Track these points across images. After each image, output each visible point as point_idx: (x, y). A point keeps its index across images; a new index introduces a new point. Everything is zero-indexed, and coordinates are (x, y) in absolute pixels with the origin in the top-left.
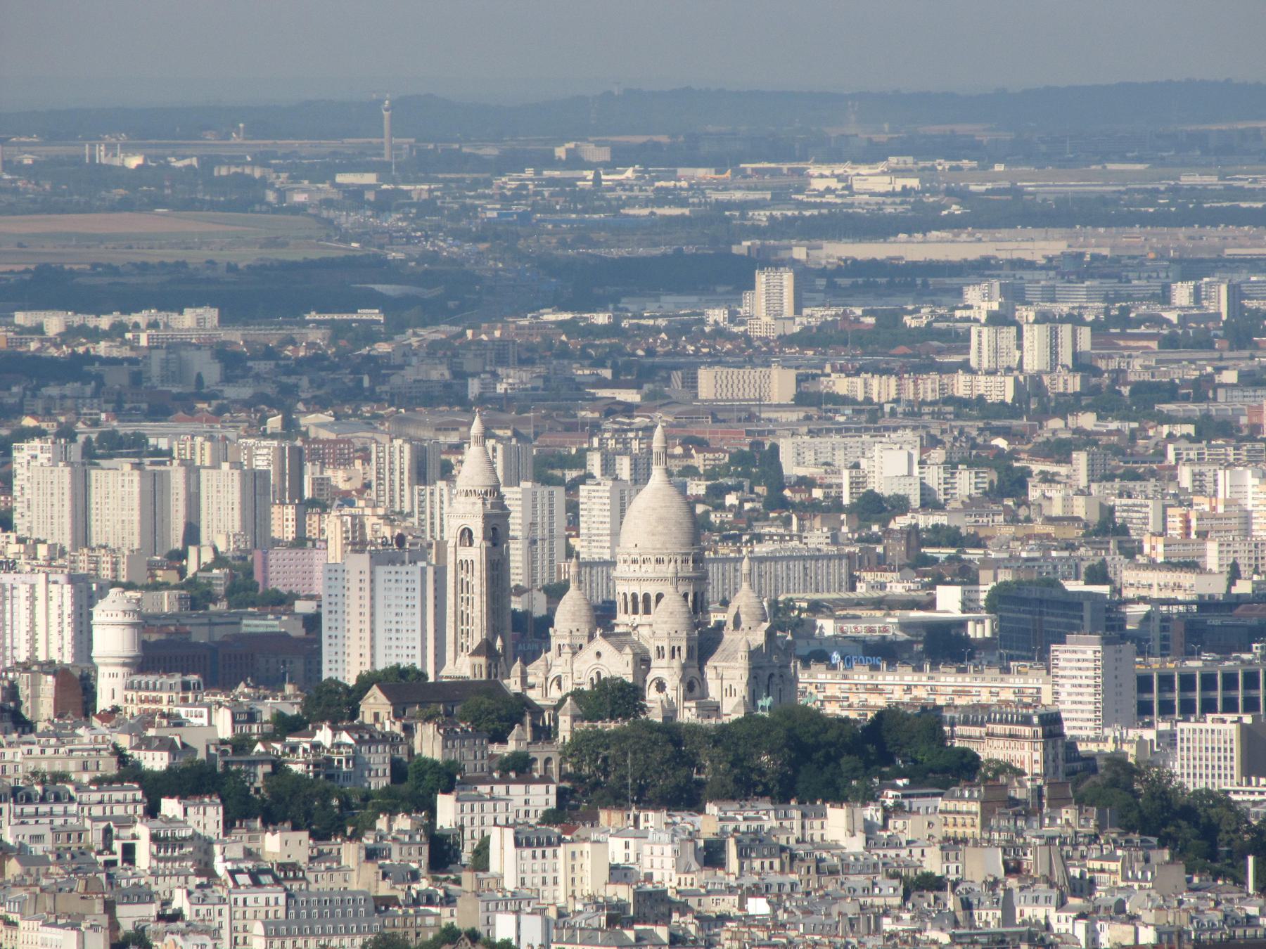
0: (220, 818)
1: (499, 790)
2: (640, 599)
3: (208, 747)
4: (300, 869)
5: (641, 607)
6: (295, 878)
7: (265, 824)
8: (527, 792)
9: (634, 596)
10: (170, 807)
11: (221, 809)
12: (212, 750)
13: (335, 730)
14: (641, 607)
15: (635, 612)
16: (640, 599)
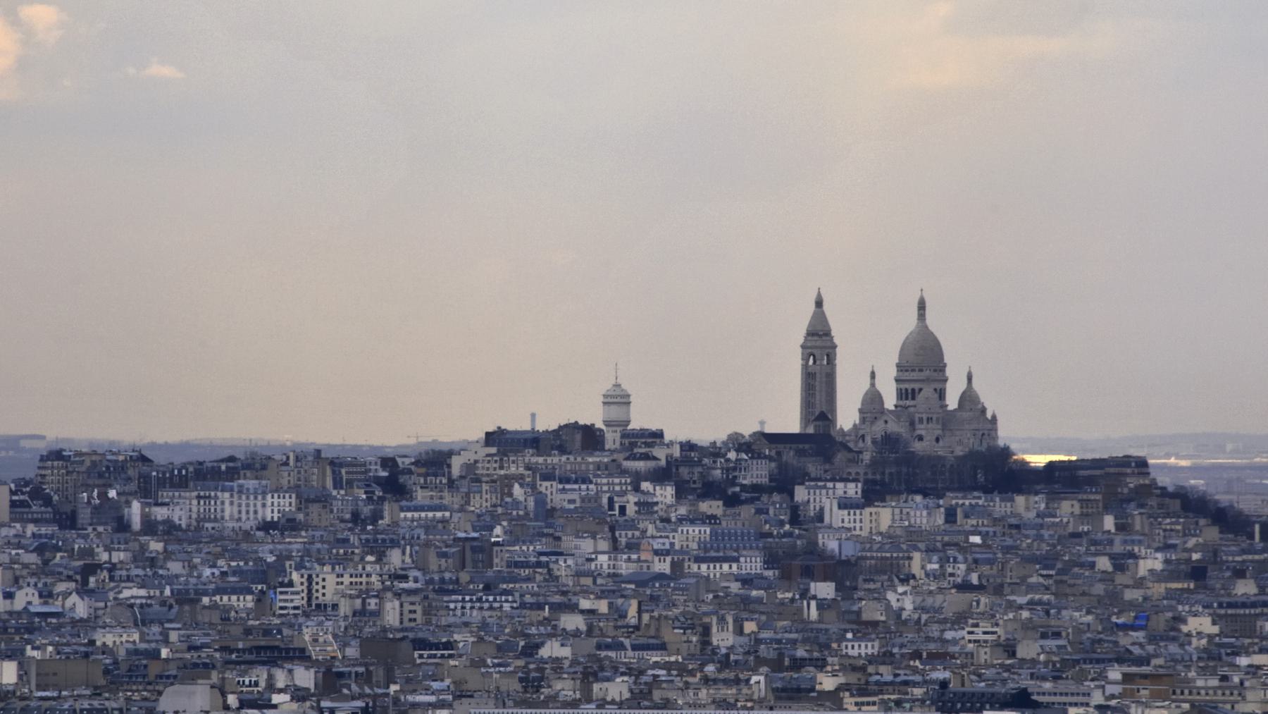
0: (674, 492)
2: (910, 391)
4: (719, 519)
5: (910, 396)
6: (715, 523)
7: (699, 496)
8: (845, 487)
14: (910, 396)
16: (910, 391)
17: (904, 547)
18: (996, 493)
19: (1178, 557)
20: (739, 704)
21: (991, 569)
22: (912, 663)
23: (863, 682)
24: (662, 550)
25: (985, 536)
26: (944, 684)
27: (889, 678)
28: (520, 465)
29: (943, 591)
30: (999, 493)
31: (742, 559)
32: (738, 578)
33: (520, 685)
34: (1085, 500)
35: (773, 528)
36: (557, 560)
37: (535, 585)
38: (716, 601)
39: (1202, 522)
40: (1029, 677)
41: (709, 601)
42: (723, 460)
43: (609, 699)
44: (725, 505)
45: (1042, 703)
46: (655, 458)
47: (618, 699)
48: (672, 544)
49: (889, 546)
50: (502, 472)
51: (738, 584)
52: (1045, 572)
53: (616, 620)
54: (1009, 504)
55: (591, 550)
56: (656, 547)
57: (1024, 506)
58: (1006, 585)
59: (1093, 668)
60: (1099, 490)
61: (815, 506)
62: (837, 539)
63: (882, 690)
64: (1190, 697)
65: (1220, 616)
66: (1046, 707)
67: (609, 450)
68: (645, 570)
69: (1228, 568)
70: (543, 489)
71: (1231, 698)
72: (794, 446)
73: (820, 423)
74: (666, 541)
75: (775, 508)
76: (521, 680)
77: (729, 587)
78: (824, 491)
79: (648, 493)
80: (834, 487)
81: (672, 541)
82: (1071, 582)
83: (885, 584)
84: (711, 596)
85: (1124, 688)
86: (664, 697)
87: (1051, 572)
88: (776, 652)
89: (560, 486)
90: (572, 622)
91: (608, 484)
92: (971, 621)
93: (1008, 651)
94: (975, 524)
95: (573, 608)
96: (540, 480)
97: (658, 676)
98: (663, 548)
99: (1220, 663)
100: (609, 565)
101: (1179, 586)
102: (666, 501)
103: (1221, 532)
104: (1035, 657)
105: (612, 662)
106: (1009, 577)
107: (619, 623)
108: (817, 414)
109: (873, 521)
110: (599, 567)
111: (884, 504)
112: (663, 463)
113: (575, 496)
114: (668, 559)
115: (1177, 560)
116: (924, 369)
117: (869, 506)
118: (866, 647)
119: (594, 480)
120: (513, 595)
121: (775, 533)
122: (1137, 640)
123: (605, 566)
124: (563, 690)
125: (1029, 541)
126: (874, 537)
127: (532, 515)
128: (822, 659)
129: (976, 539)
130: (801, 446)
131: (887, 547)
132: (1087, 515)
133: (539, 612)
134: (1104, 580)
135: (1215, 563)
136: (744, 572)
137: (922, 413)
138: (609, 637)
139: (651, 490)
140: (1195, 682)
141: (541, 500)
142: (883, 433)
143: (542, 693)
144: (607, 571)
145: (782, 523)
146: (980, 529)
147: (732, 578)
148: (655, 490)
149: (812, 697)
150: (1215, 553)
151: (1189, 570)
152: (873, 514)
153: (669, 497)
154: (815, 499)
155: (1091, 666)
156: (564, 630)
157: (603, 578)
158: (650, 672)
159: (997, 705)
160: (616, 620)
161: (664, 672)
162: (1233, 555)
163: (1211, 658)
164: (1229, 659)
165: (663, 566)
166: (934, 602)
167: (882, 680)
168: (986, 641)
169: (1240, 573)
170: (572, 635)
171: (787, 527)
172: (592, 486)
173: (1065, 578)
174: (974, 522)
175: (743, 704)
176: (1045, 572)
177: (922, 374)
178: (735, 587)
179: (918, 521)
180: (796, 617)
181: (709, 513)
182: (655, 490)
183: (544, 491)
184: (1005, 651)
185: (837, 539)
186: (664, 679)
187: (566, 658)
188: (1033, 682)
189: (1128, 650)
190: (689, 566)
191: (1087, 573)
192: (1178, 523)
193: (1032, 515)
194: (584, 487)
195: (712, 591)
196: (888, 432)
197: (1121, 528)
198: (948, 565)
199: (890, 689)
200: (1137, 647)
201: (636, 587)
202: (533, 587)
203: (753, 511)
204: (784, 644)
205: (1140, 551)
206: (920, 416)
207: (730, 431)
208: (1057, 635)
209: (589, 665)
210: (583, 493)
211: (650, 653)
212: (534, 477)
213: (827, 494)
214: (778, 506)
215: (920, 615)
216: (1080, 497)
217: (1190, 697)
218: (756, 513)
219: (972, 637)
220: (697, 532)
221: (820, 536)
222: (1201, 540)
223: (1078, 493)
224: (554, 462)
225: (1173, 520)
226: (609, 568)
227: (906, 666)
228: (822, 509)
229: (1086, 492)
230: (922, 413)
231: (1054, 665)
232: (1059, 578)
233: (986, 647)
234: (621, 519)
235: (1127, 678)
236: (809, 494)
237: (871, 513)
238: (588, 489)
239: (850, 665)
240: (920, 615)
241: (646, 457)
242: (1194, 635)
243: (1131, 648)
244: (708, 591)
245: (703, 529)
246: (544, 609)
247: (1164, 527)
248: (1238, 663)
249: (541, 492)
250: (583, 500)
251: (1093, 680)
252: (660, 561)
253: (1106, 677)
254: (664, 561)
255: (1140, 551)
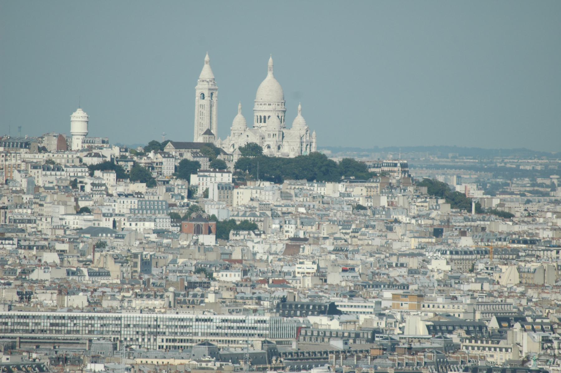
0: (115, 178)
1: (213, 174)
2: (263, 117)
3: (111, 156)
4: (143, 194)
5: (263, 120)
6: (141, 197)
7: (131, 180)
8: (222, 176)
9: (261, 117)
10: (98, 173)
11: (115, 174)
12: (112, 157)
13: (156, 153)
14: (263, 120)
15: (261, 122)
16: (263, 117)
17: (258, 214)
18: (315, 181)
19: (426, 223)
20: (156, 310)
21: (312, 228)
22: (263, 286)
23: (233, 297)
24: (108, 214)
25: (308, 208)
26: (284, 300)
27: (249, 295)
28: (18, 159)
29: (282, 241)
30: (317, 181)
31: (157, 220)
32: (155, 231)
33: (18, 297)
34: (369, 187)
35: (177, 201)
36: (41, 219)
37: (27, 234)
38: (141, 246)
39: (441, 201)
40: (335, 295)
41: (137, 245)
42: (146, 158)
43: (75, 306)
44: (147, 186)
45: (344, 312)
46: (103, 156)
47: (80, 307)
48: (114, 210)
49: (249, 213)
50: (7, 163)
51: (156, 235)
52: (344, 231)
53: (78, 257)
54: (323, 188)
55: (63, 213)
56: (104, 211)
57: (514, 196)
58: (321, 239)
59: (374, 290)
60: (378, 181)
61: (203, 188)
62: (217, 208)
63: (245, 302)
64: (433, 309)
65: (452, 260)
66: (346, 314)
67: (75, 151)
68: (96, 226)
69: (456, 229)
70: (32, 174)
71: (458, 310)
72: (190, 150)
73: (207, 136)
74: (109, 207)
75: (179, 188)
76: (18, 293)
77: (149, 237)
78: (209, 179)
79: (99, 178)
80: (215, 176)
81: (113, 207)
82: (361, 237)
83: (246, 237)
84: (138, 243)
85: (393, 303)
86: (110, 305)
87: (348, 231)
88: (179, 278)
89: (44, 173)
90: (50, 257)
91: (74, 171)
92: (299, 261)
93: (322, 279)
94: (302, 200)
95: (51, 248)
96: (31, 168)
97: (105, 292)
98: (108, 212)
99: (451, 289)
100: (74, 222)
101: (427, 240)
102: (109, 183)
103: (452, 208)
104: (339, 283)
105: (76, 283)
106: (322, 233)
107: (81, 259)
108: (205, 130)
109: (239, 197)
110: (67, 224)
111: (246, 187)
112: (108, 159)
113: (52, 179)
114: (112, 219)
115: (424, 224)
116: (272, 104)
117: (237, 188)
118: (235, 275)
119: (65, 169)
120: (13, 240)
121: (178, 204)
122: (401, 274)
123: (71, 223)
124: (46, 300)
125: (335, 211)
126: (240, 208)
127: (25, 190)
128: (208, 283)
129: (302, 210)
130: (195, 150)
131: (248, 214)
132: (370, 197)
133: (30, 251)
134: (381, 236)
135: (448, 226)
136: (158, 228)
137: (270, 131)
138: (74, 267)
139: (101, 176)
140: (436, 300)
141: (31, 182)
142: (246, 144)
143: (32, 302)
144: (73, 226)
145: (183, 198)
146: (305, 203)
147: (152, 232)
148: (103, 176)
149: (202, 306)
150: (448, 221)
151: (433, 231)
152: (239, 193)
153: (112, 180)
154: (203, 183)
155: (373, 289)
156: (46, 262)
157: (71, 230)
158: (100, 290)
159: (316, 313)
160: (78, 257)
161: (109, 290)
162: (459, 222)
163: (446, 285)
164: (457, 286)
165: (107, 224)
166: (277, 249)
167: (245, 296)
168: (308, 273)
169: (463, 233)
170: (50, 266)
171: (186, 200)
172: (63, 173)
173: (356, 235)
174: (301, 199)
175: (159, 310)
176: (344, 231)
177: (271, 107)
178: (153, 237)
179: (267, 198)
180: (191, 257)
181: (137, 191)
182: (103, 176)
183: (33, 175)
184: (320, 279)
185: (217, 208)
186: (109, 294)
187: (47, 280)
188: (338, 299)
189: (395, 280)
190: (124, 224)
191: (370, 232)
192: (425, 202)
193: (337, 195)
194: (58, 173)
195: (139, 240)
196: (249, 142)
197: (391, 204)
198: (285, 225)
199: (250, 301)
200: (401, 278)
201: (91, 236)
202: (25, 235)
203: (164, 190)
204: (184, 273)
205: (402, 219)
206: (269, 133)
207: (151, 140)
208: (353, 269)
209: (61, 284)
210: (58, 177)
211: (99, 278)
212: (27, 166)
213: (211, 180)
214: (180, 187)
215: (268, 256)
216: (366, 184)
217: (433, 309)
218: (167, 191)
219: (300, 270)
220: (129, 202)
221: (206, 206)
222: (439, 212)
223: (365, 182)
224: (40, 157)
225: (423, 200)
226: (74, 224)
227: (259, 288)
228: (207, 190)
229: (370, 182)
230: (270, 131)
231: (350, 287)
232: (353, 234)
233: (309, 276)
234: (82, 193)
235: (395, 297)
236: (199, 180)
237: (238, 193)
238: (61, 175)
239: (226, 286)
240: (268, 256)
241: (96, 155)
242: (436, 271)
243: (397, 279)
244: (136, 239)
245: (133, 201)
246: (33, 249)
247: (417, 204)
248: (462, 289)
249: (31, 176)
250: (58, 180)
251: (374, 298)
252: (106, 220)
253: (382, 296)
254: (109, 220)
255: (402, 219)
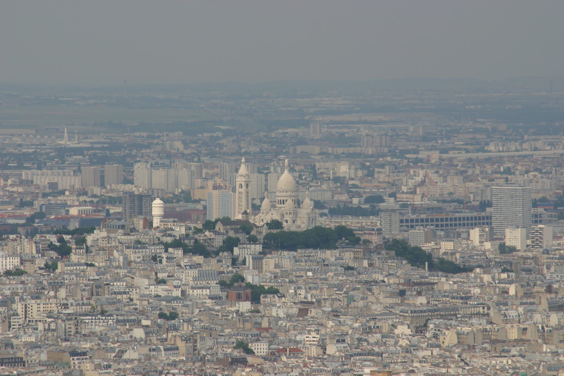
2: (282, 201)
5: (282, 203)
6: (200, 267)
7: (193, 254)
14: (282, 203)
16: (282, 201)
52: (339, 292)
55: (147, 284)
70: (126, 253)
73: (244, 215)
79: (171, 253)
87: (341, 293)
91: (154, 249)
127: (122, 266)
139: (173, 252)
145: (228, 267)
153: (180, 255)
171: (230, 268)
172: (147, 250)
176: (339, 292)
181: (197, 262)
183: (127, 254)
203: (216, 261)
218: (217, 262)
220: (192, 272)
221: (244, 274)
228: (245, 259)
241: (170, 235)
245: (195, 271)
249: (125, 254)
